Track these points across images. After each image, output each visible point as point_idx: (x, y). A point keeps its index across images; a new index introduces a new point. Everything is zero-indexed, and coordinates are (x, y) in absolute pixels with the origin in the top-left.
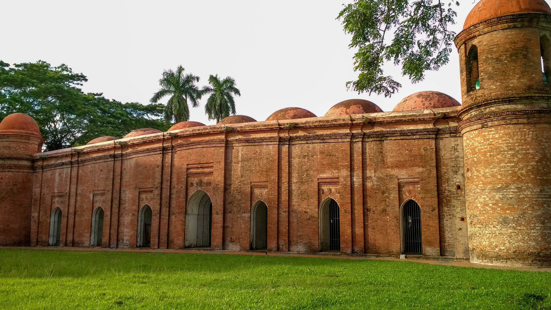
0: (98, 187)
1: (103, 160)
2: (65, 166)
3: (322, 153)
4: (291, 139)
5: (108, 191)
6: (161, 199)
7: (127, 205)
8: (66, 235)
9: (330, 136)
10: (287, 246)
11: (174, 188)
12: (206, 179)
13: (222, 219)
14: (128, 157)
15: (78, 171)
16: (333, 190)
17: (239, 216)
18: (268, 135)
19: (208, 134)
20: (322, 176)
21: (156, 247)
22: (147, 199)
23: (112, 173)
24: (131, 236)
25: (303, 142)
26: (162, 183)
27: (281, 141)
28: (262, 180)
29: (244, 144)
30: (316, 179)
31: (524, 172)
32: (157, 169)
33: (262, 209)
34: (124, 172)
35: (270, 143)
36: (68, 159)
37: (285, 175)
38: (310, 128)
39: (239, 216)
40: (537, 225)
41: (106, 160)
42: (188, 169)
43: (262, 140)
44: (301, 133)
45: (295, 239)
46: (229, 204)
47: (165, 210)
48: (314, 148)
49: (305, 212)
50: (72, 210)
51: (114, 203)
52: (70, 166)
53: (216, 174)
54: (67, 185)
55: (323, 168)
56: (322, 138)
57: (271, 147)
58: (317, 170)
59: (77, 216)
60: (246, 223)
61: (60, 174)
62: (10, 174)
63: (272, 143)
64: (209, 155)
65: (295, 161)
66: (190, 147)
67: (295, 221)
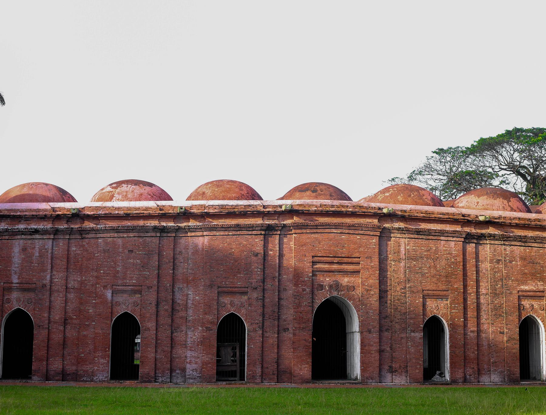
0: (125, 278)
1: (136, 234)
2: (37, 236)
3: (523, 258)
4: (482, 237)
5: (149, 288)
6: (264, 306)
7: (190, 312)
8: (47, 361)
9: (535, 239)
10: (477, 375)
11: (285, 290)
12: (345, 280)
13: (377, 340)
14: (189, 234)
15: (69, 247)
16: (536, 306)
17: (403, 335)
18: (448, 228)
19: (353, 215)
20: (522, 287)
21: (258, 380)
22: (232, 304)
23: (156, 258)
24: (204, 364)
25: (496, 242)
26: (264, 281)
27: (469, 238)
28: (440, 288)
29: (412, 236)
30: (516, 292)
32: (254, 258)
33: (433, 327)
34: (180, 258)
35: (451, 239)
36: (48, 226)
37: (471, 283)
38: (511, 226)
39: (403, 335)
41: (142, 235)
42: (314, 263)
43: (442, 233)
44: (491, 230)
45: (486, 366)
46: (385, 318)
48: (512, 252)
49: (501, 333)
50: (57, 316)
51: (161, 308)
52: (52, 236)
53: (364, 274)
54: (45, 271)
55: (524, 278)
56: (523, 240)
57: (453, 244)
58: (517, 280)
59: (68, 327)
60: (418, 346)
61: (24, 250)
63: (454, 239)
64: (352, 246)
65: (485, 266)
66: (318, 231)
67: (485, 343)
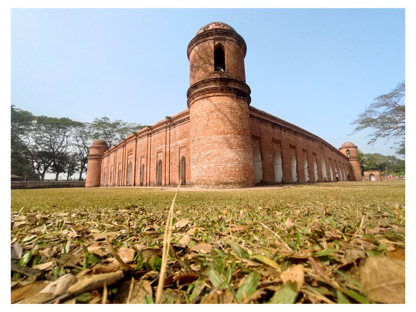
4: (151, 134)
20: (159, 149)
31: (201, 129)
40: (206, 161)
42: (128, 153)
47: (123, 170)
62: (93, 161)
